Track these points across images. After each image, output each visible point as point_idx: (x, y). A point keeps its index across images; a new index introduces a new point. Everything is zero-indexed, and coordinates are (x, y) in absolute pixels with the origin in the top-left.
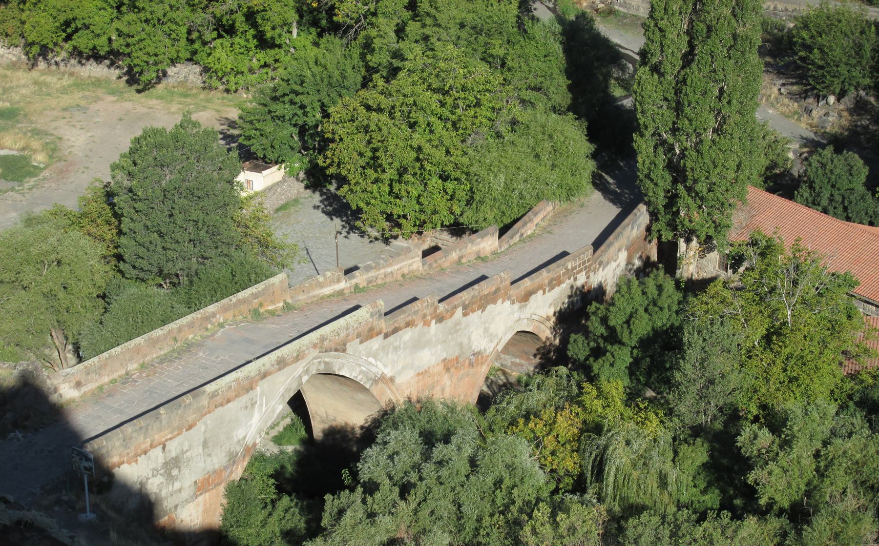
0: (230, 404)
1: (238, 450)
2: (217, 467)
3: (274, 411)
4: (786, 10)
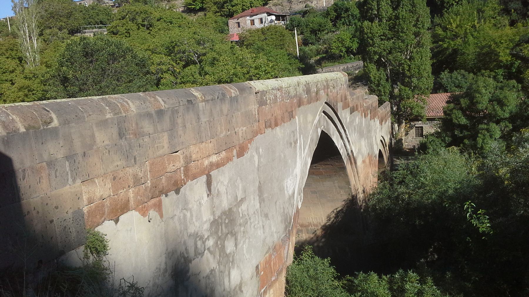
0: (278, 128)
1: (290, 212)
2: (275, 238)
3: (306, 164)
4: (353, 66)
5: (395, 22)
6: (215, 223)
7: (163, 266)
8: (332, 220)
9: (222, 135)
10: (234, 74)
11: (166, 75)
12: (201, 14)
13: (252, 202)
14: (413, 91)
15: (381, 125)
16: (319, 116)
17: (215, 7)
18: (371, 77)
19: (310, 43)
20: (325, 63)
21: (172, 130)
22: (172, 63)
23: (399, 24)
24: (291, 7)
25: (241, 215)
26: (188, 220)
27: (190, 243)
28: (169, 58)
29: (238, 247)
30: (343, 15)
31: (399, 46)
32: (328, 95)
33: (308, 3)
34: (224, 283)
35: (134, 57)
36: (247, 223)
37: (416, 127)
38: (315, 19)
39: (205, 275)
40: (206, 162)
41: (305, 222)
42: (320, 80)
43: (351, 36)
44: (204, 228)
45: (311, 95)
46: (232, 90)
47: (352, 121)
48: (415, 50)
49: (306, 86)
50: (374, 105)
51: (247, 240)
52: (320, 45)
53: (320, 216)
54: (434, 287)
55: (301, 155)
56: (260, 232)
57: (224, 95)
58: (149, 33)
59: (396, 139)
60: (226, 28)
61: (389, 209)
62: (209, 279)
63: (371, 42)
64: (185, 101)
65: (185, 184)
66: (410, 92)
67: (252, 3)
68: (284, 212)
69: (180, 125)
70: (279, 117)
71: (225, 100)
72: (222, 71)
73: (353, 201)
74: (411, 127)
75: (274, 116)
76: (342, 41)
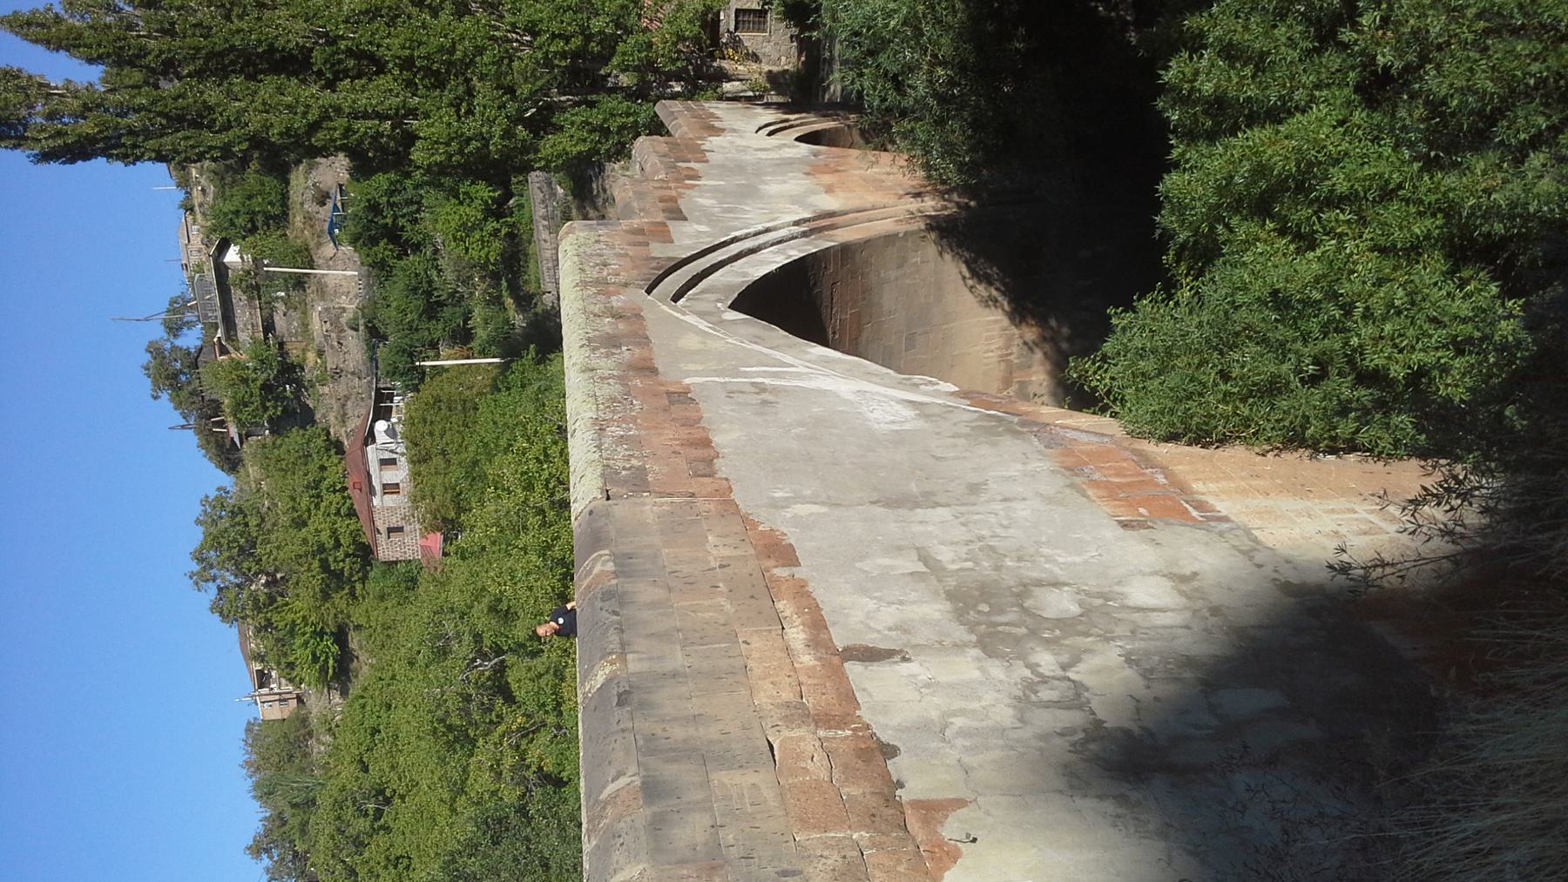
0: (717, 439)
1: (966, 416)
3: (827, 362)
5: (419, 69)
6: (990, 643)
7: (1109, 807)
8: (995, 293)
9: (728, 607)
10: (542, 554)
11: (532, 756)
12: (354, 641)
13: (930, 528)
14: (629, 32)
15: (723, 130)
16: (686, 314)
17: (336, 597)
18: (580, 153)
19: (465, 322)
20: (526, 282)
21: (707, 757)
22: (495, 736)
23: (427, 58)
24: (353, 373)
25: (969, 564)
26: (975, 724)
27: (1046, 720)
28: (481, 742)
29: (1062, 579)
30: (389, 221)
31: (494, 63)
32: (626, 285)
33: (343, 321)
34: (1164, 627)
35: (472, 848)
36: (992, 548)
37: (736, 29)
38: (394, 304)
39: (1141, 682)
40: (807, 659)
41: (998, 371)
42: (579, 305)
43: (453, 201)
44: (1002, 677)
45: (624, 334)
46: (594, 569)
47: (709, 218)
48: (509, 18)
49: (594, 350)
50: (664, 148)
51: (1045, 551)
52: (472, 294)
53: (982, 328)
54: (1215, 9)
55: (798, 376)
56: (1022, 511)
57: (608, 595)
58: (402, 797)
59: (766, 90)
60: (401, 568)
61: (975, 124)
62: (1152, 671)
63: (474, 144)
64: (620, 713)
65: (868, 727)
66: (631, 41)
67: (334, 485)
68: (966, 436)
69: (692, 731)
70: (684, 433)
71: (625, 593)
72: (531, 589)
73: (945, 230)
74: (736, 43)
75: (678, 448)
76: (467, 229)
